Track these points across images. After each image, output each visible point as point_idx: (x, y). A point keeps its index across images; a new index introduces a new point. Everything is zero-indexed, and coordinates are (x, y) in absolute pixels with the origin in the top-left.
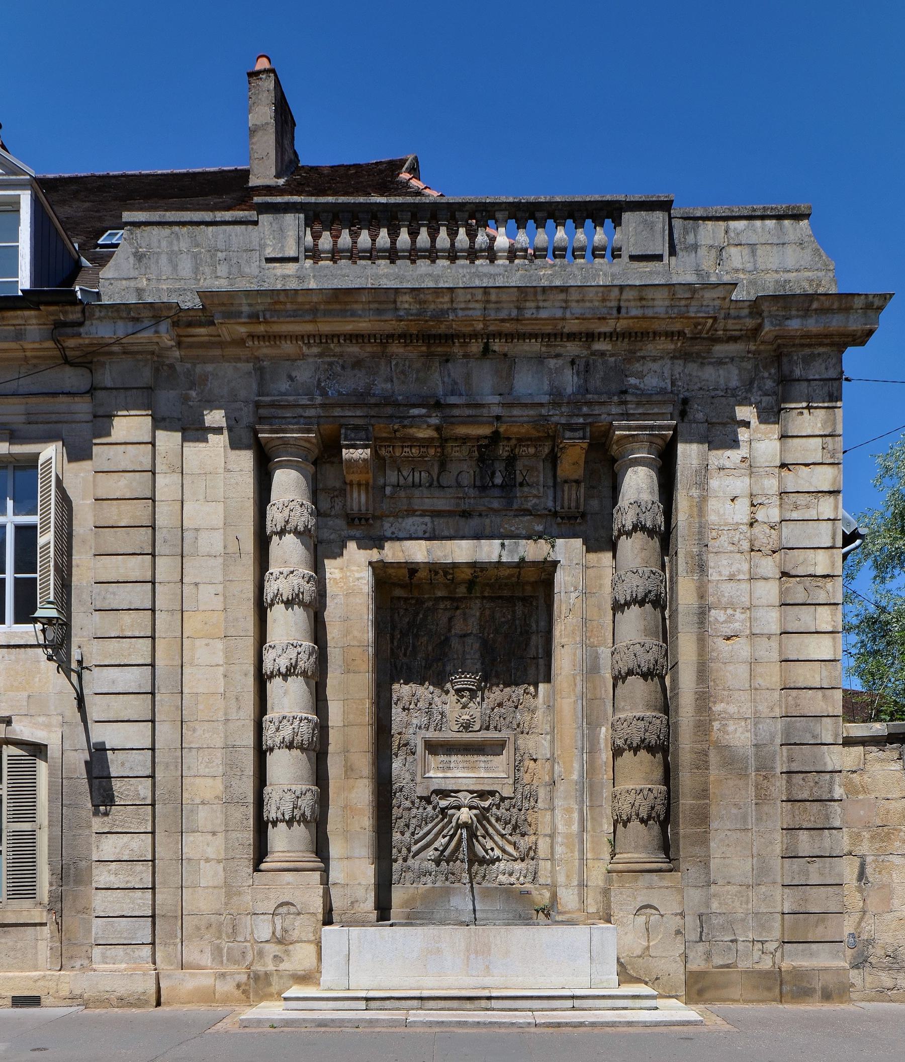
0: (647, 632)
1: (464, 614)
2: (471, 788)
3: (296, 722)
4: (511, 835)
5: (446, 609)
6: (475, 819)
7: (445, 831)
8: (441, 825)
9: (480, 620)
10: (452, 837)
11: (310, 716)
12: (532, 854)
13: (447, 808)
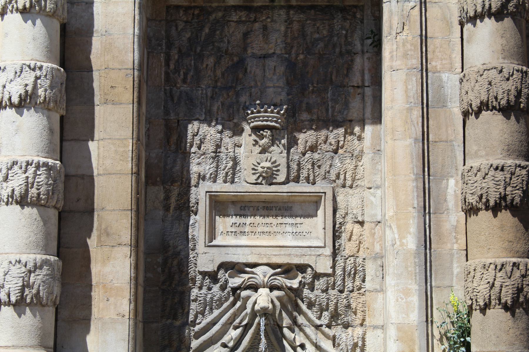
0: (506, 54)
1: (265, 28)
3: (31, 170)
4: (329, 326)
5: (239, 22)
6: (277, 303)
7: (238, 321)
8: (231, 311)
9: (286, 36)
10: (247, 328)
11: (51, 161)
13: (239, 288)
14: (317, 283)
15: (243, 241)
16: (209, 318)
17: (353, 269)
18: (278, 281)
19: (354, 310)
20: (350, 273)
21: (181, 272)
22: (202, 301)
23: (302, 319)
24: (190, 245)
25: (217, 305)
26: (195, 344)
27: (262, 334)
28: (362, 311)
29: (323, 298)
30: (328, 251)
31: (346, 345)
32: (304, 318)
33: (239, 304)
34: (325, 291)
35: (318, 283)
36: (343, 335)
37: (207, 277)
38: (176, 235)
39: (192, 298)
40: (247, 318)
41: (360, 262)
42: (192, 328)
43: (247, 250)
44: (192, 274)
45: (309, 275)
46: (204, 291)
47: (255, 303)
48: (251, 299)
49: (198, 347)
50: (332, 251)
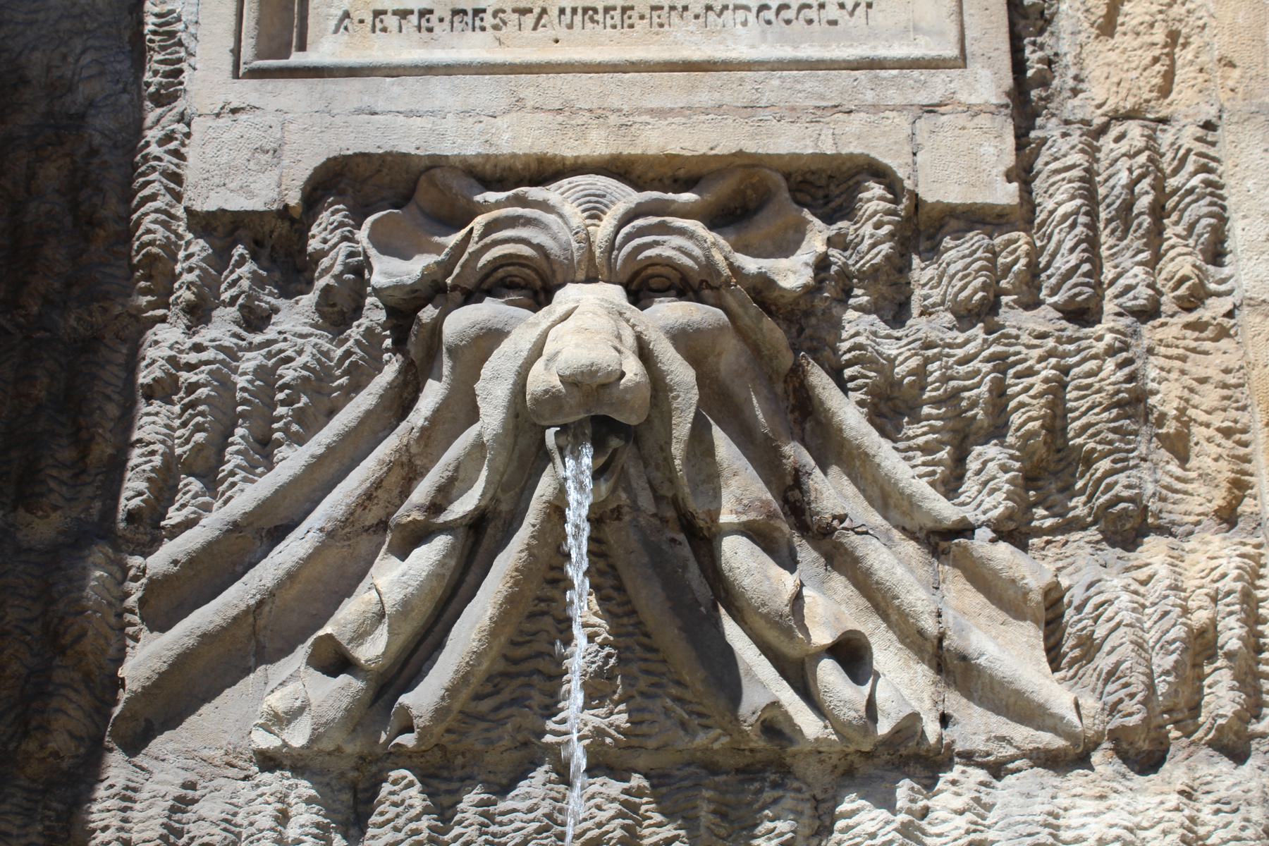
2: (657, 140)
4: (1014, 531)
6: (680, 372)
7: (422, 492)
8: (387, 448)
10: (480, 537)
12: (1221, 697)
13: (435, 290)
14: (921, 272)
15: (473, 47)
16: (246, 497)
17: (1145, 184)
18: (677, 241)
19: (1171, 427)
20: (1128, 206)
21: (86, 223)
22: (203, 392)
23: (841, 494)
24: (148, 77)
25: (300, 416)
26: (146, 657)
27: (577, 570)
28: (1227, 433)
29: (962, 362)
30: (987, 83)
31: (1139, 645)
32: (850, 489)
33: (432, 394)
34: (978, 313)
35: (931, 271)
36: (1114, 583)
37: (239, 250)
38: (66, 24)
39: (144, 377)
40: (484, 473)
41: (1187, 142)
42: (136, 561)
43: (486, 90)
44: (150, 228)
45: (872, 227)
46: (221, 328)
47: (537, 351)
48: (506, 346)
49: (163, 676)
50: (1008, 82)
